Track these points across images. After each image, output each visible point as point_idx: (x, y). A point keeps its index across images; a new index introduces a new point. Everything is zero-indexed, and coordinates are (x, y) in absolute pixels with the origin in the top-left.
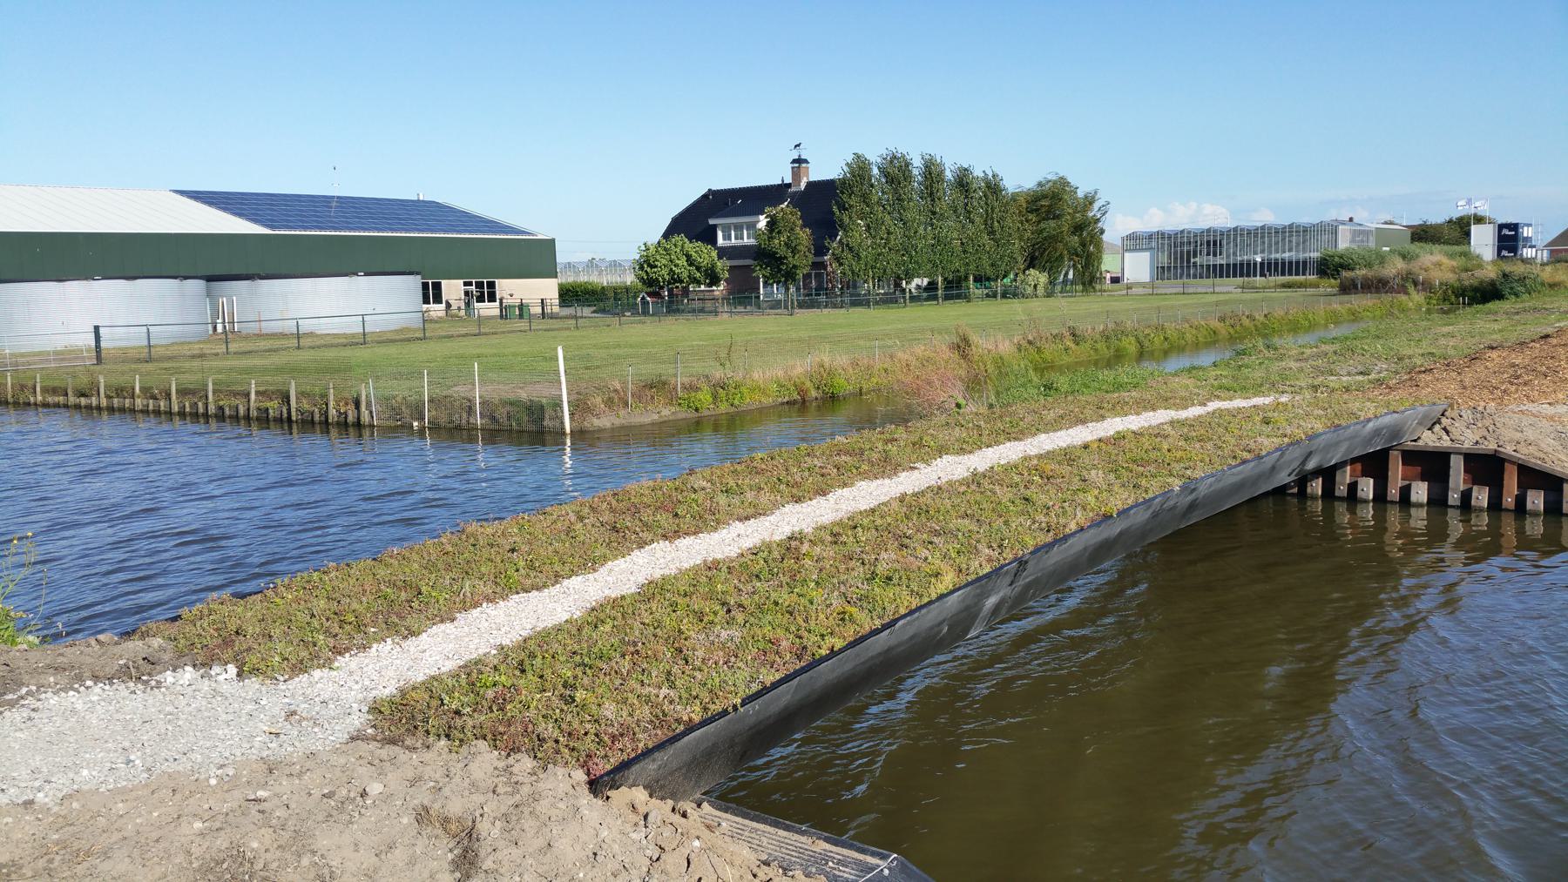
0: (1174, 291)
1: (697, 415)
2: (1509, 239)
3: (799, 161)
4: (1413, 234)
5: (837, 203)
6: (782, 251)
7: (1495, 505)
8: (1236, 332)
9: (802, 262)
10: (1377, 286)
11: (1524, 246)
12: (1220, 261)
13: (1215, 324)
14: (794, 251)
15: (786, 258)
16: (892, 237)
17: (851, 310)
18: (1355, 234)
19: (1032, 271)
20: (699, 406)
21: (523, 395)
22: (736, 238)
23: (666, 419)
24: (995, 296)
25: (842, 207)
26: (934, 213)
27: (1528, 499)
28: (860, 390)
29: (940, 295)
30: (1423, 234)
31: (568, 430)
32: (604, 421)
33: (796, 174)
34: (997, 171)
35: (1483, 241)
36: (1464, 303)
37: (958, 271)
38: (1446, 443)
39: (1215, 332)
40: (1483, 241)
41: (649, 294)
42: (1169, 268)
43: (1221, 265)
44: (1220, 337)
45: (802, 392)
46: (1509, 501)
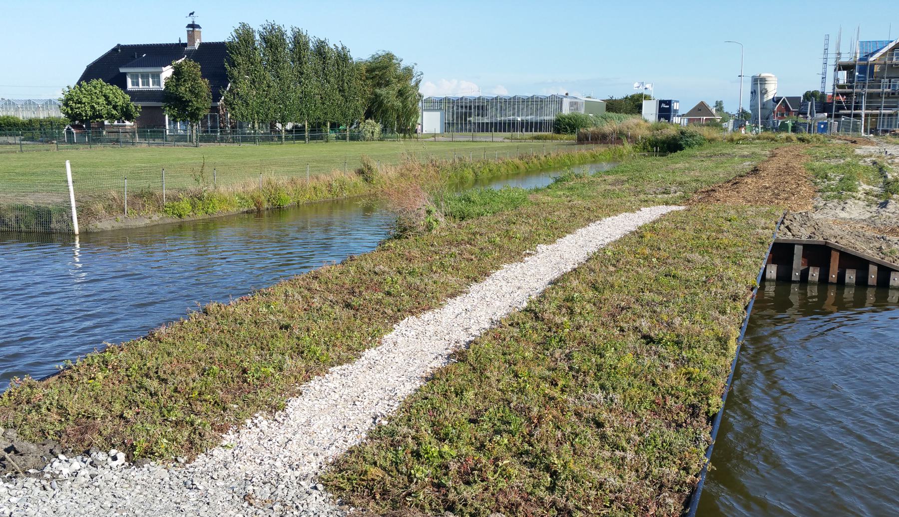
0: (467, 139)
1: (180, 220)
2: (665, 110)
3: (193, 26)
4: (607, 105)
5: (228, 61)
6: (188, 96)
7: (824, 279)
8: (530, 168)
9: (203, 105)
10: (600, 138)
11: (674, 116)
12: (486, 120)
13: (517, 161)
14: (197, 95)
15: (190, 101)
16: (272, 90)
17: (242, 145)
18: (572, 104)
19: (369, 121)
20: (182, 213)
21: (30, 201)
22: (143, 85)
23: (156, 223)
24: (344, 138)
25: (233, 64)
26: (302, 74)
27: (847, 275)
28: (298, 203)
29: (306, 136)
30: (612, 106)
31: (77, 231)
32: (105, 224)
33: (191, 36)
34: (345, 44)
35: (650, 110)
36: (656, 151)
37: (319, 118)
38: (789, 237)
39: (517, 167)
40: (650, 110)
41: (74, 126)
42: (453, 123)
43: (487, 123)
44: (521, 171)
45: (258, 204)
46: (833, 277)
